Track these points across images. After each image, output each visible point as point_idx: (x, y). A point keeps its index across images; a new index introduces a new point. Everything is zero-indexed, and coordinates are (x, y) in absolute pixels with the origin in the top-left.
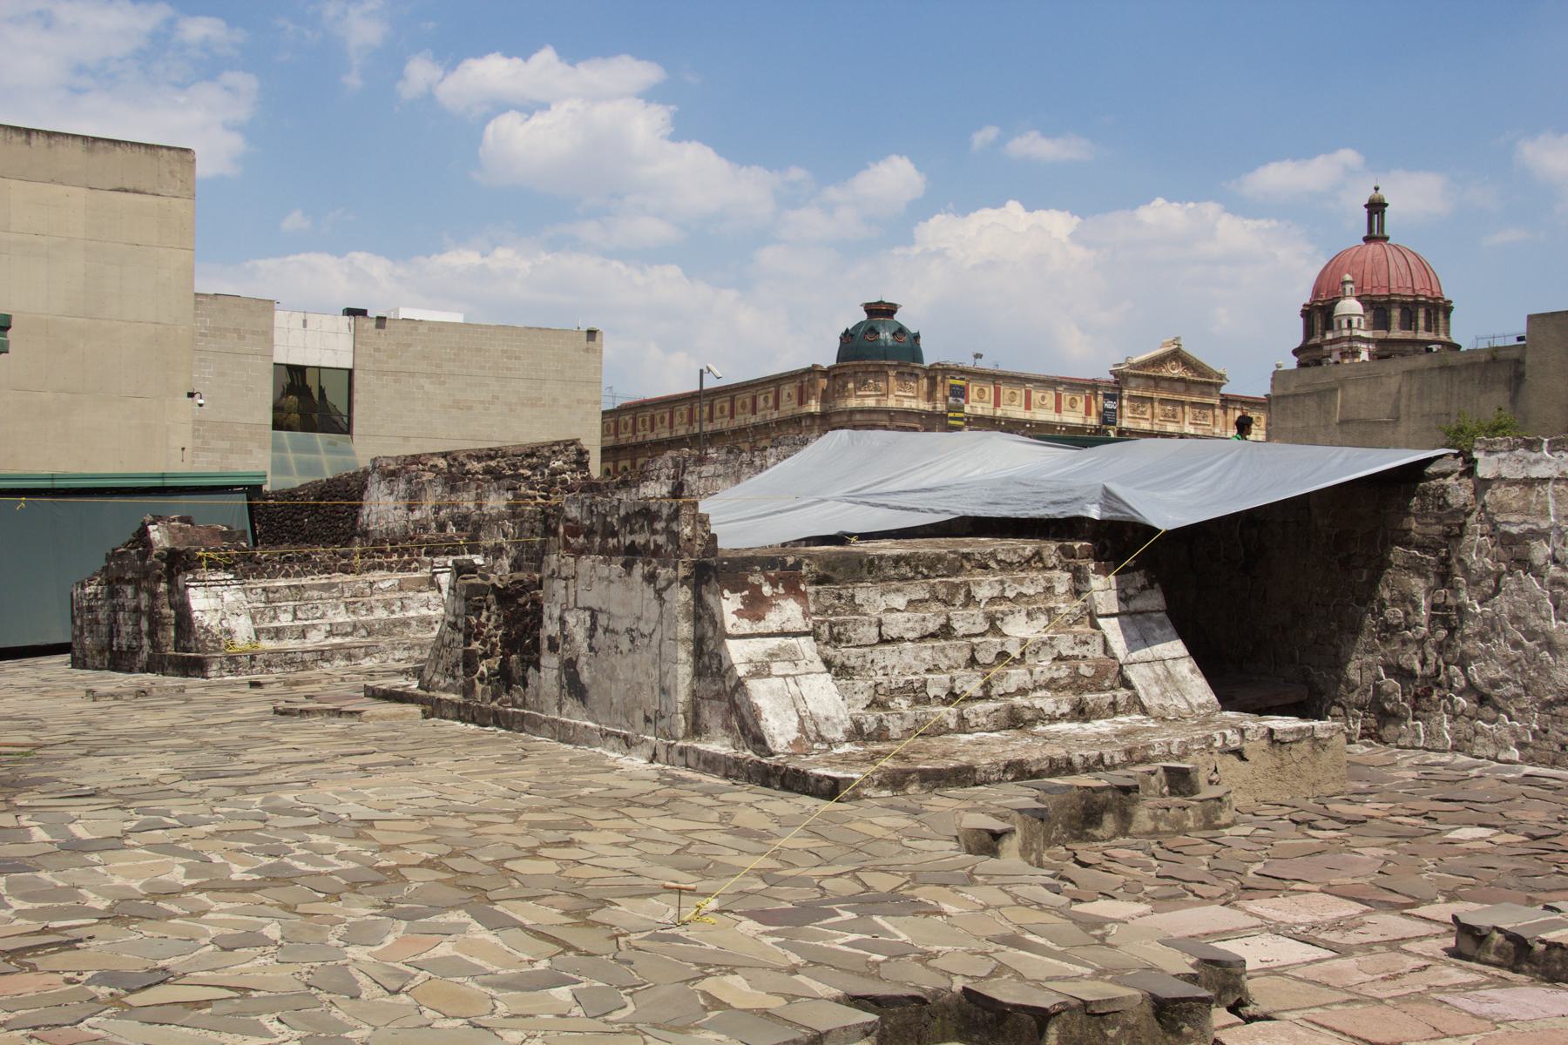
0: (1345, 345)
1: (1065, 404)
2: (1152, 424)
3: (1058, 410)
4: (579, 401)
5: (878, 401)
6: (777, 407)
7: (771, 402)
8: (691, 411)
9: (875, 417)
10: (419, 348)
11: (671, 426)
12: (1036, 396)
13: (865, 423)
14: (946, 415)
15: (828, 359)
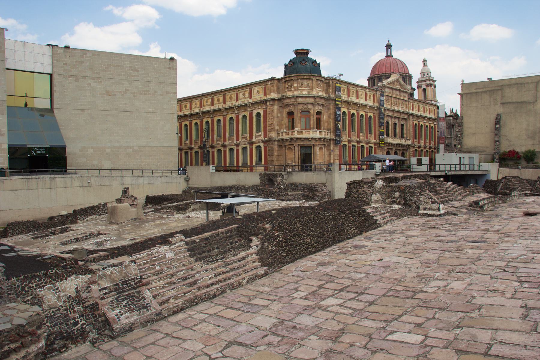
0: (428, 82)
1: (368, 98)
2: (391, 107)
3: (366, 100)
4: (167, 93)
5: (309, 92)
6: (251, 97)
7: (247, 95)
8: (201, 102)
9: (308, 99)
10: (88, 64)
11: (191, 109)
12: (360, 93)
13: (303, 102)
14: (335, 99)
15: (280, 74)
